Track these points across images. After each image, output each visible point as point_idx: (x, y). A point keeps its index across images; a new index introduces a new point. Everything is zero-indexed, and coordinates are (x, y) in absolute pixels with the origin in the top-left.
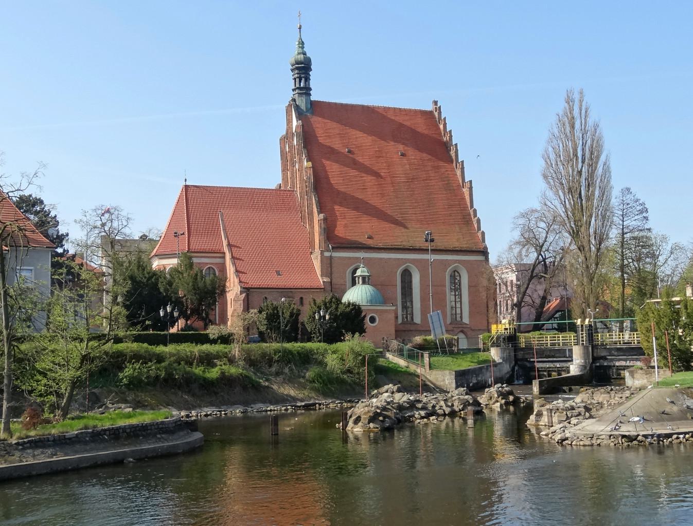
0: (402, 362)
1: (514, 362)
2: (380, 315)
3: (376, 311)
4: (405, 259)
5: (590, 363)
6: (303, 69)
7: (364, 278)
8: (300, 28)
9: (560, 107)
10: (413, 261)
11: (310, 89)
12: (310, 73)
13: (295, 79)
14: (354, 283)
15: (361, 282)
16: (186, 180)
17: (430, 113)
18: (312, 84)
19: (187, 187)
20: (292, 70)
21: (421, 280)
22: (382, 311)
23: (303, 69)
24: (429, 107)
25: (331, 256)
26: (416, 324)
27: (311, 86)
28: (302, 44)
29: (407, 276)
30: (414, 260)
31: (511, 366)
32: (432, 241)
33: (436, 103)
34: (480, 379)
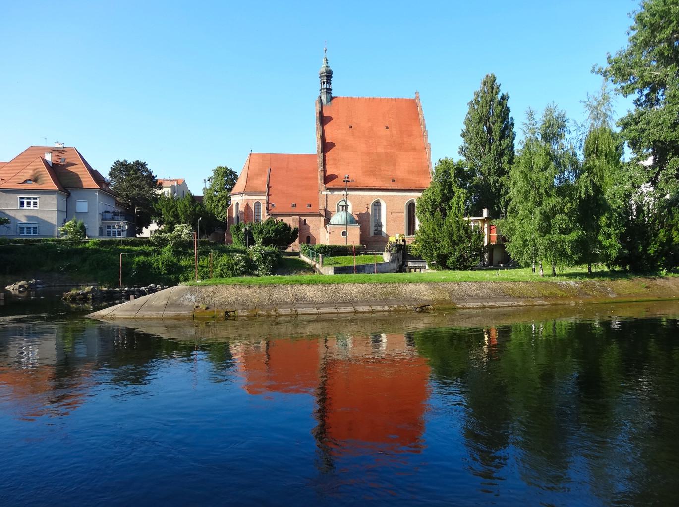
0: (307, 260)
4: (376, 195)
7: (343, 207)
9: (478, 86)
10: (382, 197)
11: (331, 90)
14: (338, 211)
15: (341, 210)
17: (414, 100)
18: (332, 87)
20: (320, 77)
24: (412, 96)
26: (382, 237)
30: (383, 196)
31: (399, 265)
32: (347, 181)
33: (417, 93)
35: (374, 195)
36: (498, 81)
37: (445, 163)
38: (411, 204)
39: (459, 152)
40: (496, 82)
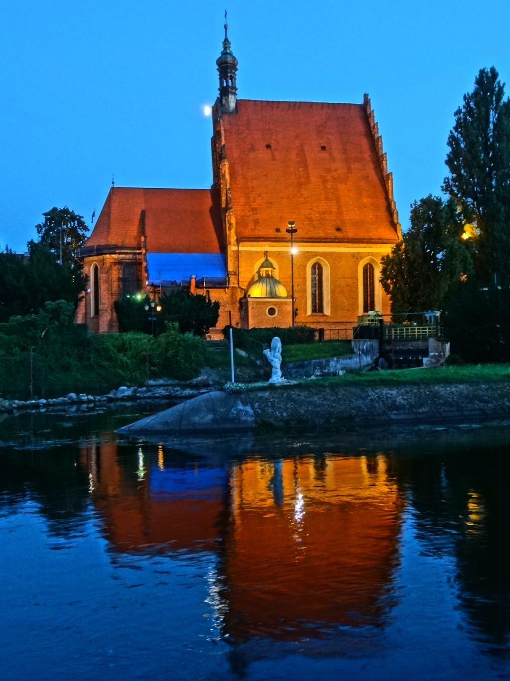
1: (378, 354)
2: (280, 307)
3: (275, 304)
4: (315, 252)
5: (447, 356)
6: (226, 67)
8: (226, 27)
9: (471, 88)
10: (325, 255)
12: (236, 73)
13: (220, 79)
16: (113, 183)
18: (238, 84)
19: (113, 188)
21: (331, 273)
22: (281, 303)
23: (226, 67)
24: (361, 101)
25: (238, 250)
26: (325, 315)
27: (237, 86)
28: (226, 43)
29: (318, 269)
31: (375, 358)
33: (366, 96)
34: (326, 371)
35: (311, 252)
36: (501, 78)
37: (429, 204)
38: (367, 264)
39: (442, 187)
40: (498, 80)
